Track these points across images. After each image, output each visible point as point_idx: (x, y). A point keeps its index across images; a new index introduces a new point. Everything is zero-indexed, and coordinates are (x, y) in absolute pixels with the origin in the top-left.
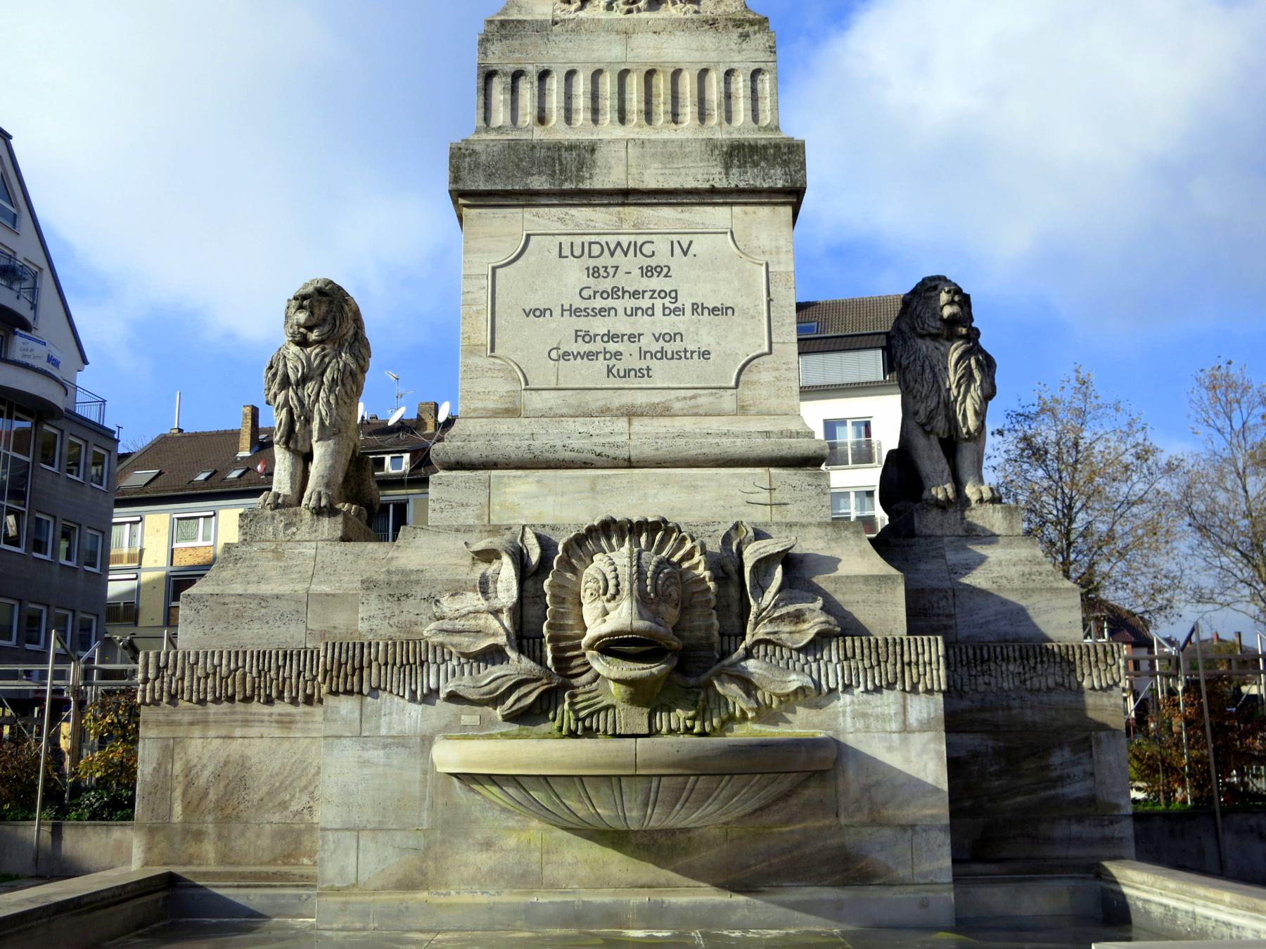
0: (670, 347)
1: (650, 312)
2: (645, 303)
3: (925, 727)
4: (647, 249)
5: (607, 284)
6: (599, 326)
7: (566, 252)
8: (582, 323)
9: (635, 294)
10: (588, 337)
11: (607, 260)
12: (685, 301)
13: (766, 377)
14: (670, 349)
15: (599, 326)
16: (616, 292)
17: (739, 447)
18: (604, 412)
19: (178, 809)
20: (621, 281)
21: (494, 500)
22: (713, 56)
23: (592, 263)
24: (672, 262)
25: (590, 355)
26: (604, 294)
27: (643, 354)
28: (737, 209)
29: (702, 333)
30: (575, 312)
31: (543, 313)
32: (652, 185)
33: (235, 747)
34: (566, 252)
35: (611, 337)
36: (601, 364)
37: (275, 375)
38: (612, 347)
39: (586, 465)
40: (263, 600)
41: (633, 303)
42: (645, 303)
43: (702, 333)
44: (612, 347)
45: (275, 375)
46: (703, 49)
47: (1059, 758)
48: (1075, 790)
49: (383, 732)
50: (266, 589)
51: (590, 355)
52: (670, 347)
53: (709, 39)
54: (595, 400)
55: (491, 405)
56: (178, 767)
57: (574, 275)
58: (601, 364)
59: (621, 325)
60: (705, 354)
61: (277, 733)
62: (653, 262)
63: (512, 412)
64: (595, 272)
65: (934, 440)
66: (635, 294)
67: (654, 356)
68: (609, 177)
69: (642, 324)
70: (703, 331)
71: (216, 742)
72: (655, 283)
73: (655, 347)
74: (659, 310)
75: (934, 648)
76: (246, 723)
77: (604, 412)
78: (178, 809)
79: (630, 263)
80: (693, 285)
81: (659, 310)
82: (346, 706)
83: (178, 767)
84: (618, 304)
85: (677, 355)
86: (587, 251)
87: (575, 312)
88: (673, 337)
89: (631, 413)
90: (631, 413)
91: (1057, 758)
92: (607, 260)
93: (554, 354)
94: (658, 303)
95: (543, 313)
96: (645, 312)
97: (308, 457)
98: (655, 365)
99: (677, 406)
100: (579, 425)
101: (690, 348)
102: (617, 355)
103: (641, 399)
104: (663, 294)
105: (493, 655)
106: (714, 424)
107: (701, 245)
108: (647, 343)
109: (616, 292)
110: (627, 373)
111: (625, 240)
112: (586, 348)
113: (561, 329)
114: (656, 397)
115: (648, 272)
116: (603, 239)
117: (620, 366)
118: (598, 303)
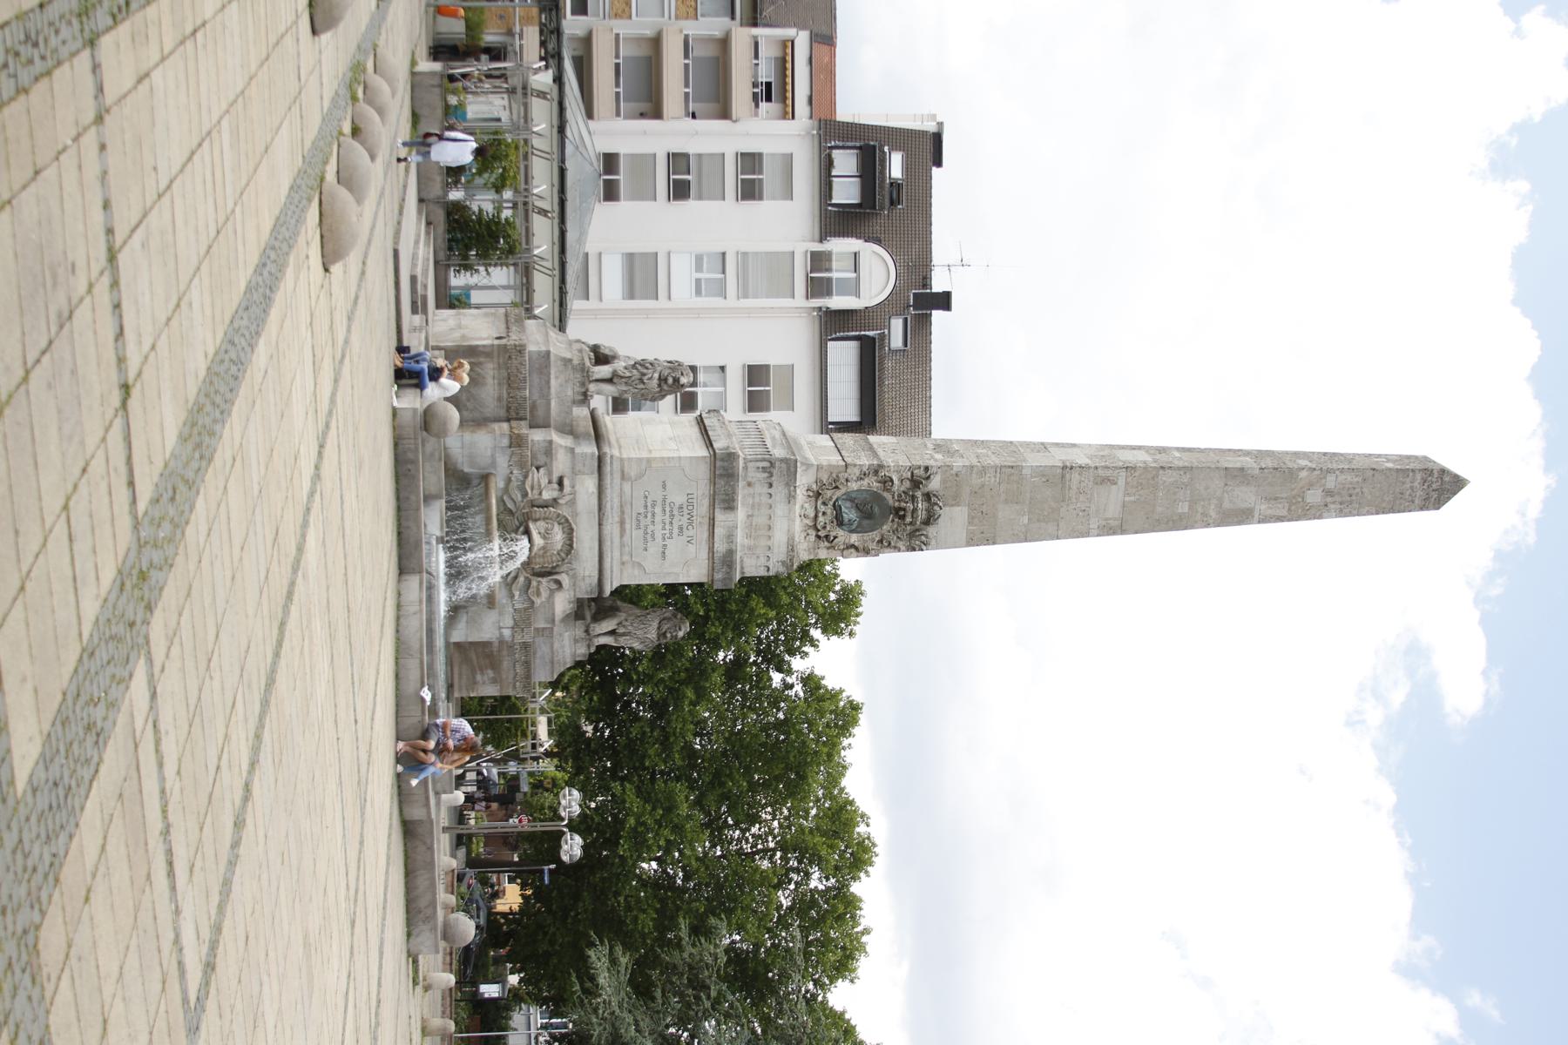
3: (501, 635)
6: (658, 510)
8: (659, 503)
10: (653, 506)
12: (668, 542)
14: (648, 536)
15: (658, 510)
16: (672, 516)
17: (607, 565)
18: (623, 512)
29: (654, 548)
33: (490, 381)
39: (600, 509)
40: (548, 382)
43: (654, 548)
47: (490, 673)
48: (479, 677)
50: (553, 382)
53: (784, 549)
54: (627, 510)
57: (679, 499)
59: (658, 518)
63: (623, 477)
64: (681, 507)
68: (720, 516)
72: (676, 531)
77: (623, 512)
80: (674, 546)
82: (506, 442)
89: (622, 523)
90: (622, 523)
97: (610, 381)
100: (616, 501)
103: (628, 526)
105: (525, 495)
106: (617, 554)
109: (672, 516)
113: (657, 495)
115: (681, 528)
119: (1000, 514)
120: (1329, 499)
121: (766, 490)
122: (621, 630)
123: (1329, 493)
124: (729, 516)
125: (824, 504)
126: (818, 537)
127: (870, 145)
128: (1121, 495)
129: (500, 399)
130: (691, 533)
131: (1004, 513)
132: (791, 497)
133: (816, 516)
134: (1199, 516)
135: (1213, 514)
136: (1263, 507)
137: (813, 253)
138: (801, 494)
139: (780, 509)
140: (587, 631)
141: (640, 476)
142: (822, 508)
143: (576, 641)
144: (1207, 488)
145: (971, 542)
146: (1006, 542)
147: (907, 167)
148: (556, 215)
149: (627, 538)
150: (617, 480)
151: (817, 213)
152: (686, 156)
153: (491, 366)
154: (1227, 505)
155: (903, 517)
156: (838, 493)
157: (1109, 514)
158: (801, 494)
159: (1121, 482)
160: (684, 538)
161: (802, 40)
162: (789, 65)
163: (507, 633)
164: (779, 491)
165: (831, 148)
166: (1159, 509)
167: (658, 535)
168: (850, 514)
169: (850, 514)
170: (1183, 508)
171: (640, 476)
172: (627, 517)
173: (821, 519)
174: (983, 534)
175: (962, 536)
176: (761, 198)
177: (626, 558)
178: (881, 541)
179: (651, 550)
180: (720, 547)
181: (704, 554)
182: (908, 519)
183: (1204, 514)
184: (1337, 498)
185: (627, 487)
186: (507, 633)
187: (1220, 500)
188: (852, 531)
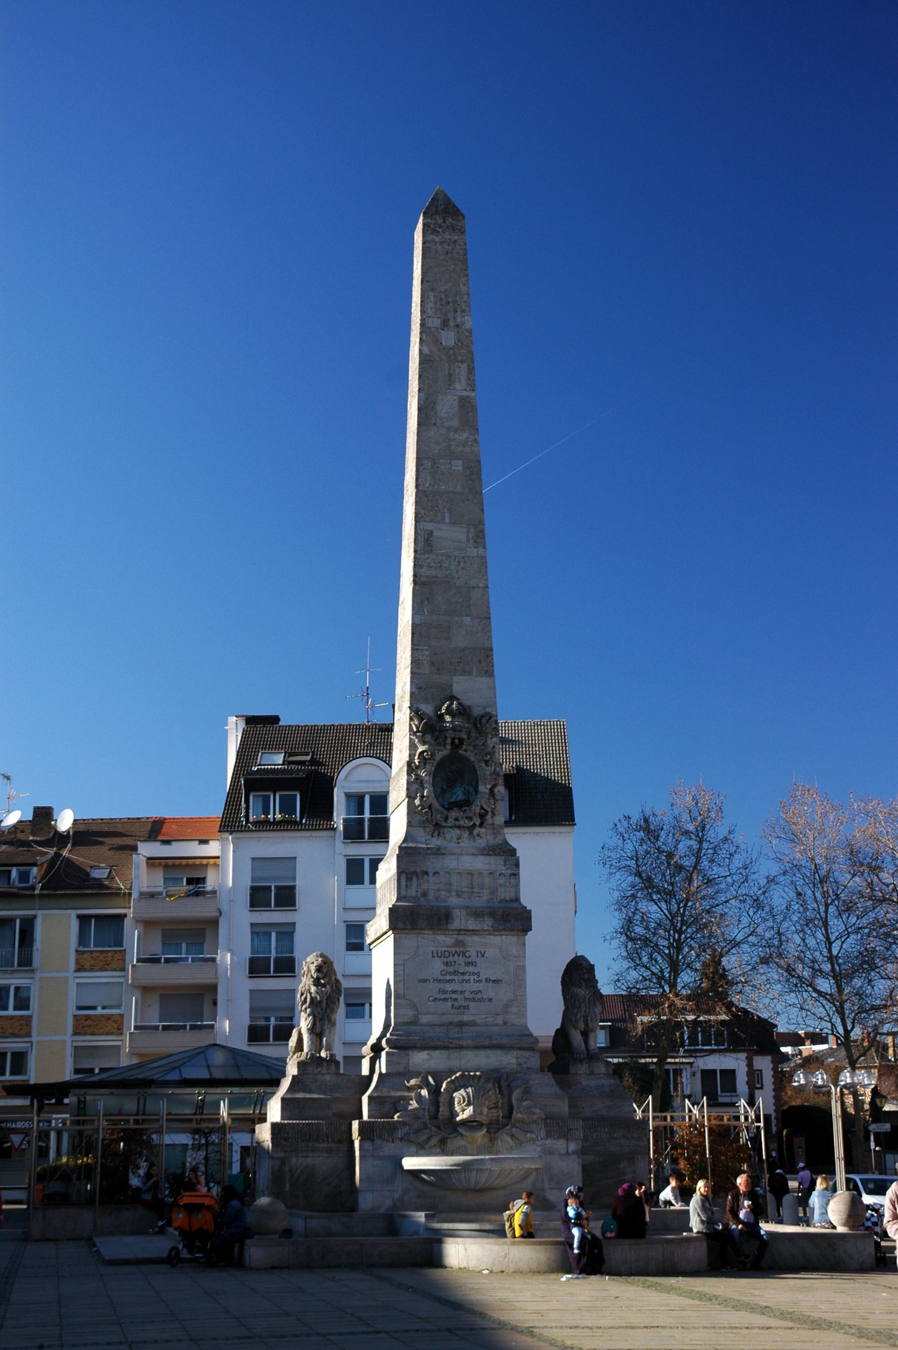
0: (477, 997)
1: (468, 981)
2: (467, 978)
3: (575, 1152)
4: (467, 954)
5: (451, 969)
6: (449, 987)
7: (435, 955)
8: (441, 986)
9: (463, 974)
10: (444, 992)
11: (451, 959)
13: (514, 1010)
14: (477, 998)
15: (449, 987)
19: (288, 1185)
20: (456, 968)
21: (411, 1062)
22: (494, 867)
23: (445, 960)
24: (478, 960)
25: (445, 1000)
26: (450, 974)
27: (466, 999)
28: (503, 937)
30: (439, 981)
31: (426, 981)
32: (471, 928)
34: (435, 955)
35: (454, 992)
36: (449, 1003)
37: (306, 999)
38: (454, 996)
41: (461, 977)
42: (467, 978)
43: (490, 992)
44: (454, 996)
45: (306, 999)
46: (489, 864)
47: (623, 1164)
49: (381, 1154)
51: (445, 1000)
52: (477, 997)
53: (492, 859)
54: (447, 1019)
55: (406, 1020)
56: (287, 1169)
57: (438, 965)
58: (449, 1003)
59: (459, 987)
60: (490, 1000)
61: (326, 1155)
62: (469, 960)
64: (446, 964)
65: (578, 1031)
66: (463, 974)
67: (470, 1000)
69: (466, 986)
70: (490, 990)
71: (301, 1159)
72: (471, 969)
73: (471, 996)
74: (472, 981)
75: (580, 1124)
76: (313, 1151)
78: (288, 1185)
79: (461, 960)
80: (486, 971)
81: (472, 981)
83: (287, 1169)
84: (456, 978)
85: (480, 1000)
86: (441, 955)
87: (439, 981)
88: (477, 993)
91: (622, 1165)
92: (451, 959)
93: (431, 999)
94: (472, 978)
95: (426, 981)
96: (466, 981)
98: (471, 1004)
99: (479, 1021)
101: (485, 997)
102: (456, 999)
103: (466, 1018)
104: (474, 974)
107: (490, 952)
108: (467, 994)
109: (455, 973)
110: (460, 1007)
111: (457, 949)
112: (443, 996)
113: (432, 988)
114: (471, 1018)
115: (468, 964)
116: (450, 949)
117: (456, 1004)
118: (448, 977)
119: (461, 645)
120: (452, 323)
121: (432, 879)
122: (582, 1025)
123: (445, 324)
124: (456, 913)
125: (446, 819)
126: (481, 825)
127: (251, 782)
128: (444, 527)
129: (329, 1151)
130: (475, 954)
131: (460, 641)
132: (438, 852)
133: (459, 827)
134: (467, 449)
135: (465, 436)
136: (460, 387)
137: (346, 837)
138: (436, 842)
139: (451, 863)
140: (581, 1061)
141: (413, 1006)
142: (451, 821)
143: (591, 1073)
144: (438, 443)
145: (489, 672)
146: (490, 638)
147: (273, 747)
148: (82, 1091)
149: (480, 1019)
150: (417, 1028)
151: (308, 834)
152: (252, 961)
153: (294, 1160)
154: (456, 423)
155: (461, 740)
156: (436, 805)
157: (463, 537)
158: (436, 842)
159: (430, 526)
160: (479, 960)
161: (147, 849)
162: (170, 862)
163: (572, 1147)
164: (432, 864)
165: (247, 821)
166: (459, 488)
167: (475, 987)
168: (459, 794)
169: (459, 794)
170: (458, 465)
171: (413, 1006)
172: (456, 1019)
173: (462, 823)
174: (482, 661)
175: (484, 680)
176: (293, 888)
177: (500, 1020)
178: (486, 762)
179: (491, 994)
180: (487, 923)
181: (497, 940)
182: (464, 736)
183: (465, 443)
184: (450, 316)
185: (424, 1019)
186: (572, 1147)
187: (449, 429)
188: (476, 791)
